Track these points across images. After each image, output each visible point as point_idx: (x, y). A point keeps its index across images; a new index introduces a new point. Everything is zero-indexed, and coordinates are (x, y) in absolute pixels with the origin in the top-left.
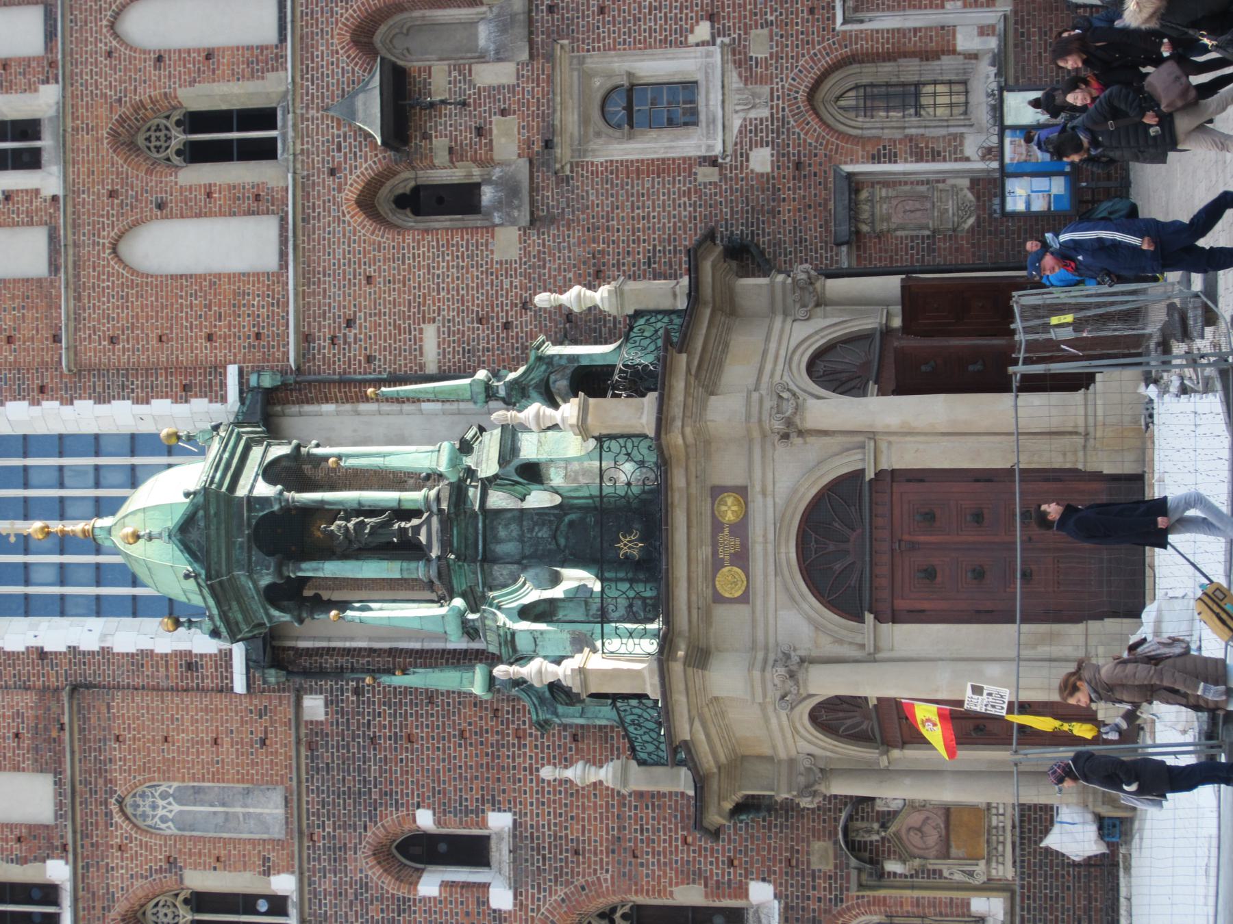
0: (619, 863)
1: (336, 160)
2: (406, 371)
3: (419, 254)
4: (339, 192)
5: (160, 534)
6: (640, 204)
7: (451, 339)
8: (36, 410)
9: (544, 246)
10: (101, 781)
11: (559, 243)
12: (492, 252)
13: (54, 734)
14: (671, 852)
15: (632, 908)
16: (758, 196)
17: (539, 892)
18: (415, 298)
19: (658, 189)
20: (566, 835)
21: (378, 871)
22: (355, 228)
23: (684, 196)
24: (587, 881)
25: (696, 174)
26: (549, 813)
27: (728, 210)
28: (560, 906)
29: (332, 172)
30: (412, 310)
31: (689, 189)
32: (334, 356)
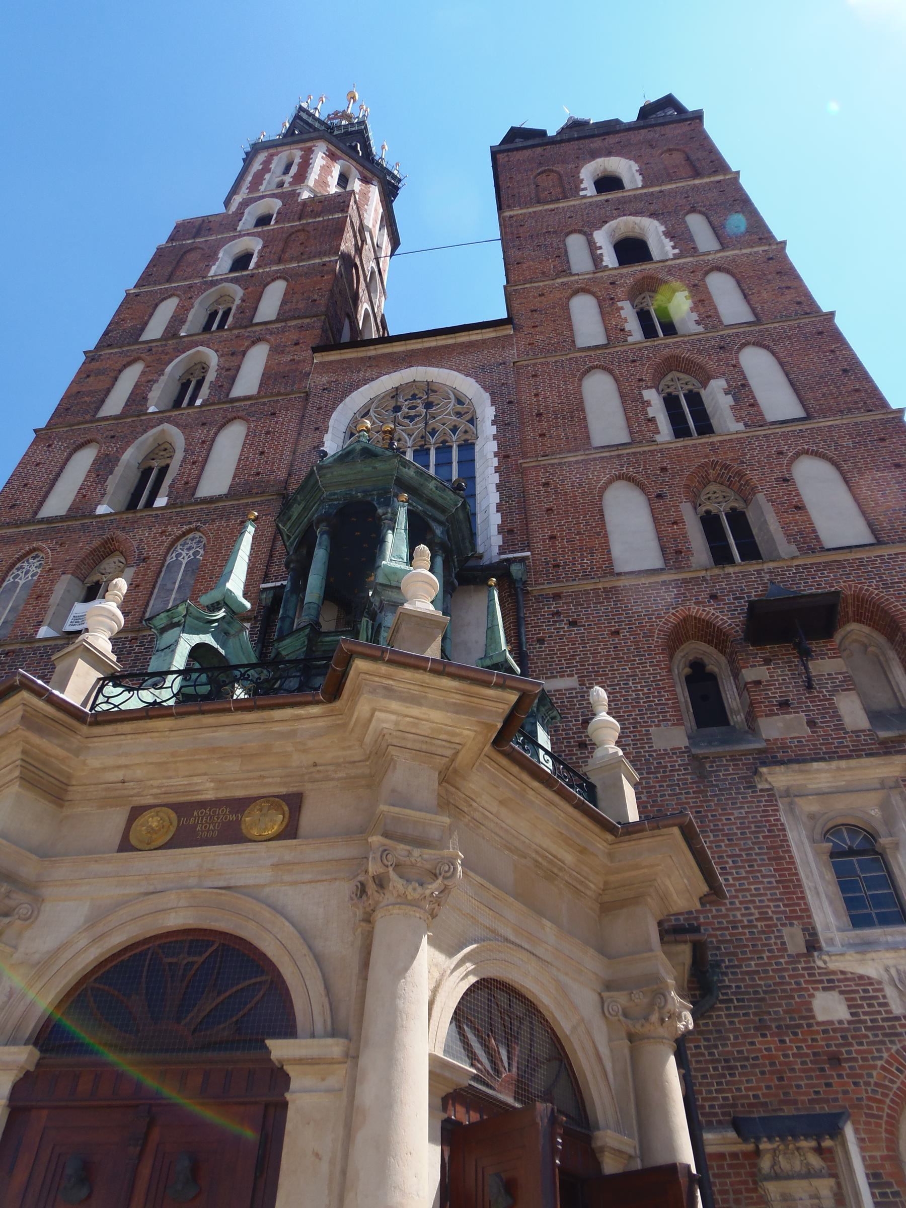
1: (726, 598)
2: (531, 668)
3: (646, 667)
6: (740, 864)
7: (565, 700)
9: (671, 771)
10: (215, 516)
11: (678, 785)
12: (658, 726)
16: (780, 1005)
18: (603, 667)
19: (762, 883)
22: (663, 617)
23: (760, 913)
25: (792, 925)
27: (754, 968)
29: (713, 597)
30: (590, 667)
31: (771, 919)
32: (541, 615)
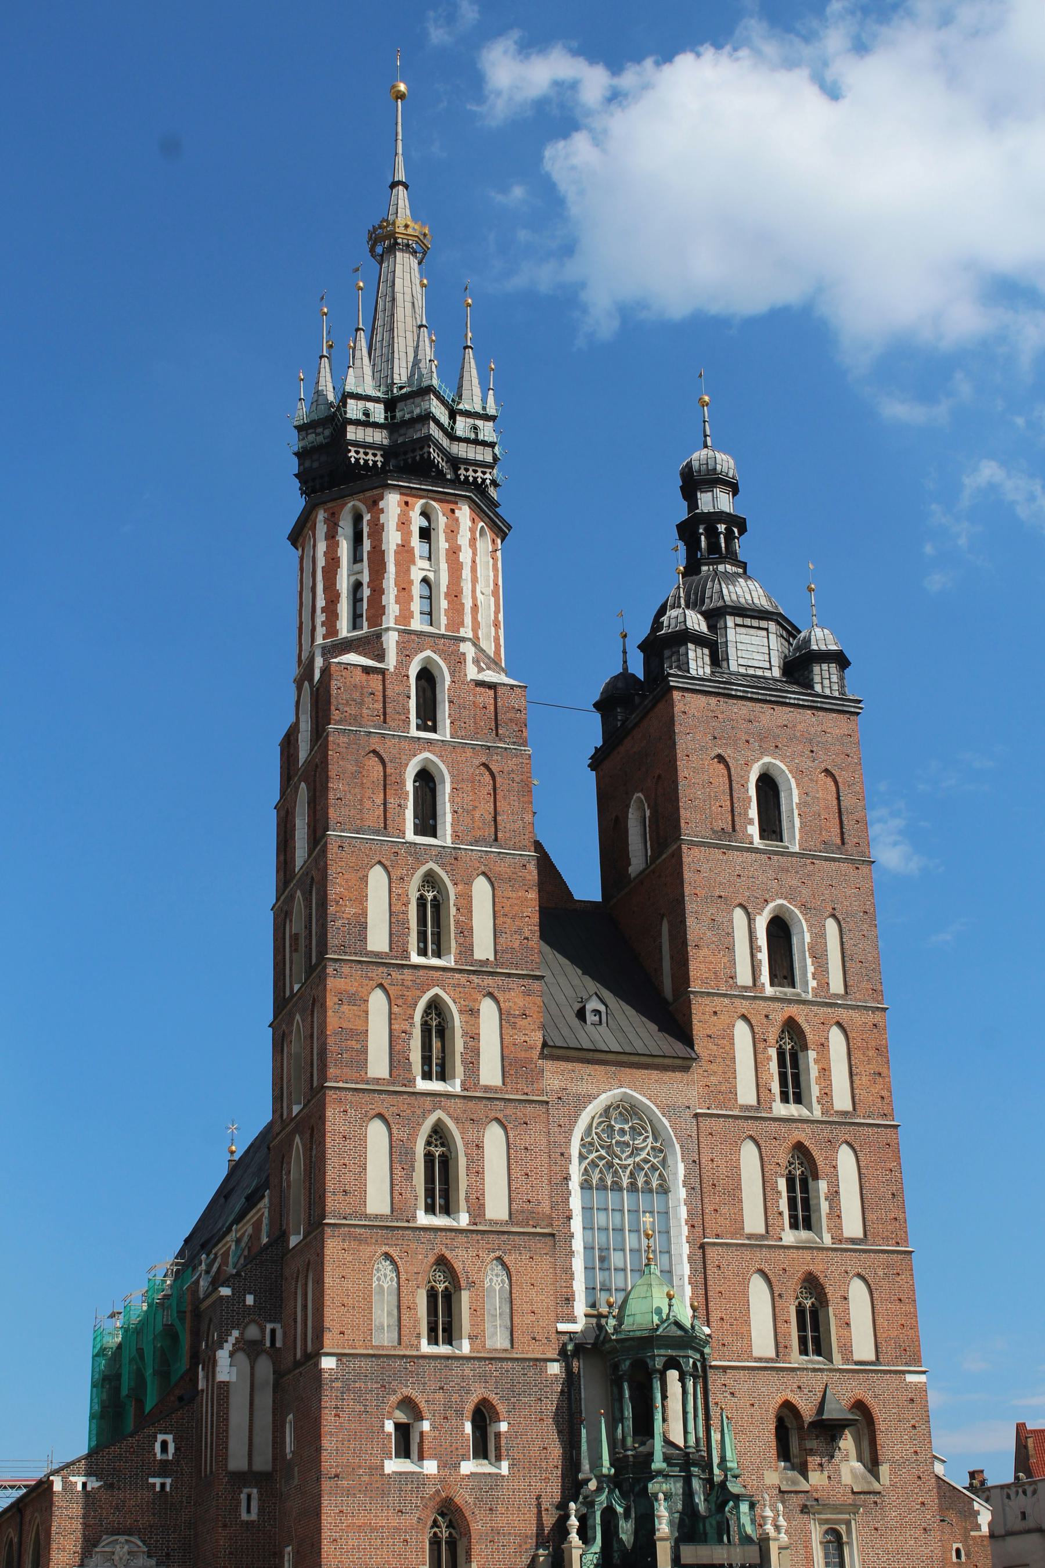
0: (487, 1533)
4: (791, 1391)
5: (673, 1311)
8: (683, 1223)
10: (510, 1247)
12: (767, 1470)
13: (531, 1223)
14: (493, 1561)
15: (455, 1538)
17: (470, 1489)
20: (499, 1504)
21: (476, 1400)
24: (477, 1515)
26: (509, 1495)
28: (463, 1500)
29: (799, 1387)
